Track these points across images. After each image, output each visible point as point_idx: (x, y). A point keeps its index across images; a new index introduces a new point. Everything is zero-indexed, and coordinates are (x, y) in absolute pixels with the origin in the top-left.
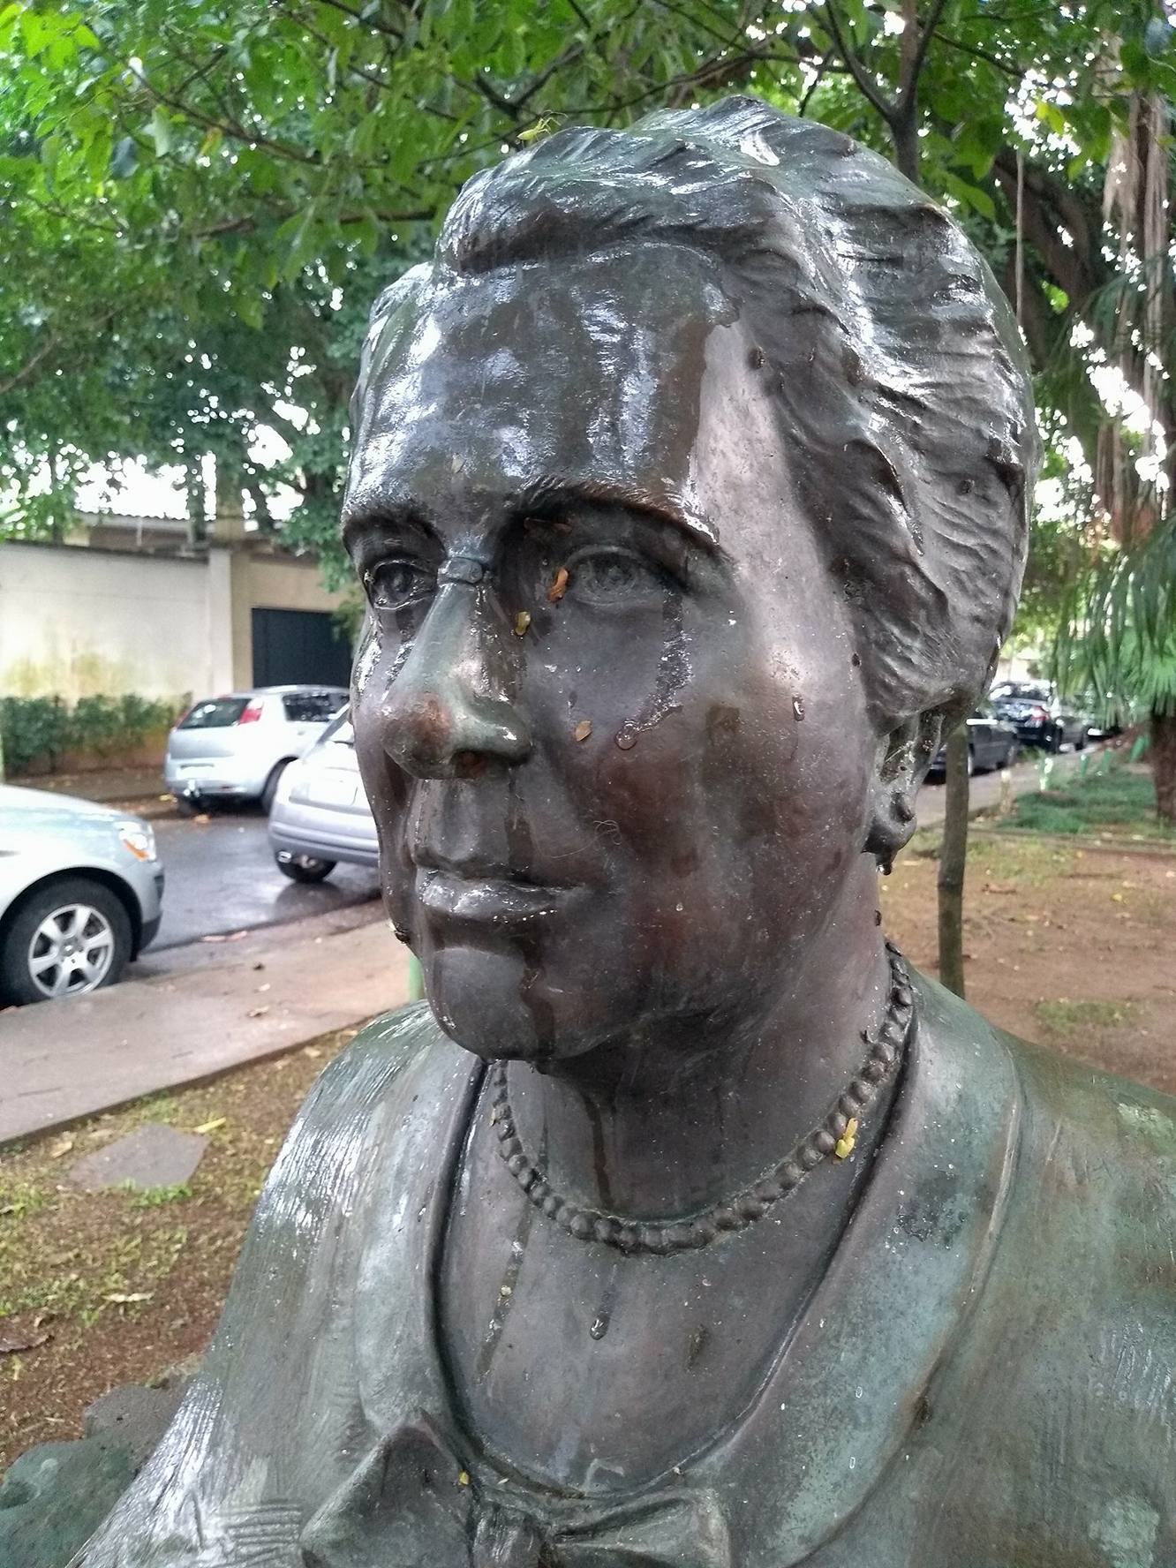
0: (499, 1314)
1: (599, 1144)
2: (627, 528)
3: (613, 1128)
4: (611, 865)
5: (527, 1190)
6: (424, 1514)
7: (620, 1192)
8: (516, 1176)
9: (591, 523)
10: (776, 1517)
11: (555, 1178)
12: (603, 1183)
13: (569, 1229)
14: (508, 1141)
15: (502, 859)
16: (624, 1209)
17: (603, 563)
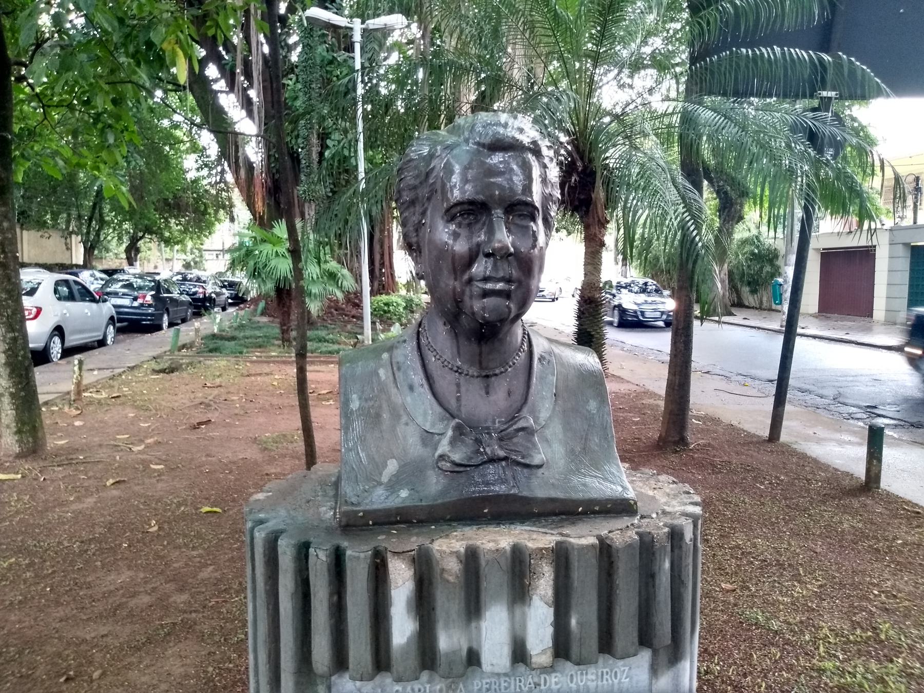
0: (458, 399)
1: (480, 354)
2: (530, 209)
3: (485, 348)
4: (523, 278)
5: (456, 371)
6: (463, 441)
7: (484, 364)
8: (451, 369)
9: (523, 208)
10: (538, 418)
11: (465, 367)
12: (480, 363)
13: (473, 376)
14: (446, 363)
15: (508, 277)
16: (486, 368)
17: (520, 215)
